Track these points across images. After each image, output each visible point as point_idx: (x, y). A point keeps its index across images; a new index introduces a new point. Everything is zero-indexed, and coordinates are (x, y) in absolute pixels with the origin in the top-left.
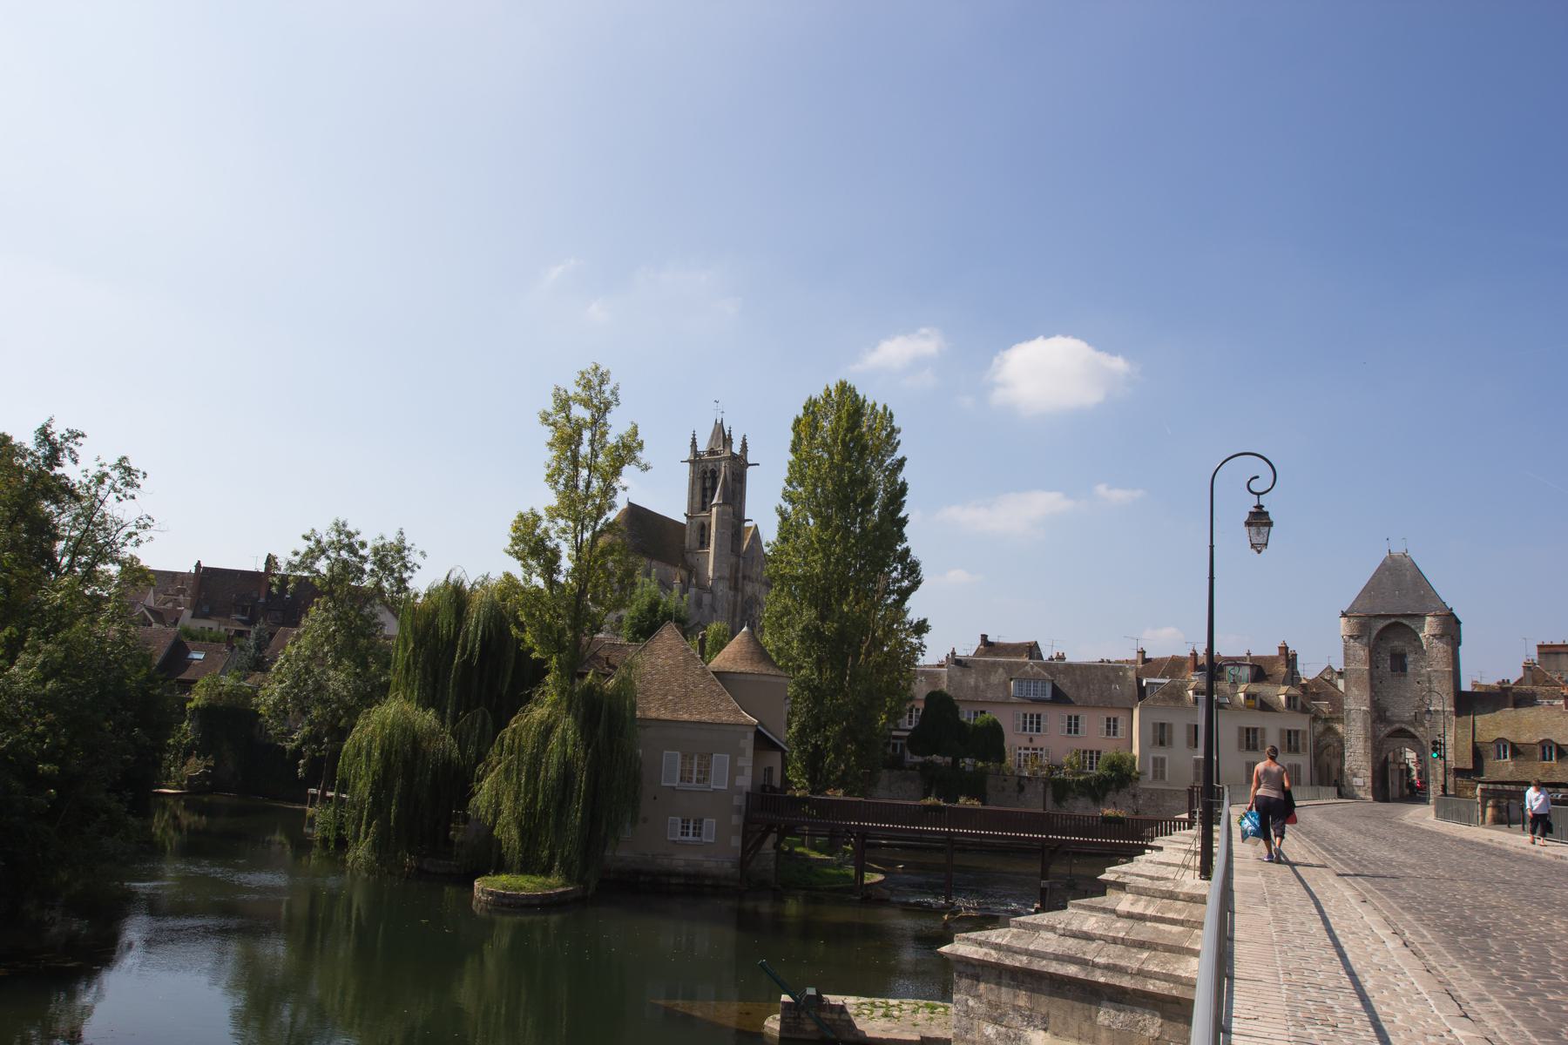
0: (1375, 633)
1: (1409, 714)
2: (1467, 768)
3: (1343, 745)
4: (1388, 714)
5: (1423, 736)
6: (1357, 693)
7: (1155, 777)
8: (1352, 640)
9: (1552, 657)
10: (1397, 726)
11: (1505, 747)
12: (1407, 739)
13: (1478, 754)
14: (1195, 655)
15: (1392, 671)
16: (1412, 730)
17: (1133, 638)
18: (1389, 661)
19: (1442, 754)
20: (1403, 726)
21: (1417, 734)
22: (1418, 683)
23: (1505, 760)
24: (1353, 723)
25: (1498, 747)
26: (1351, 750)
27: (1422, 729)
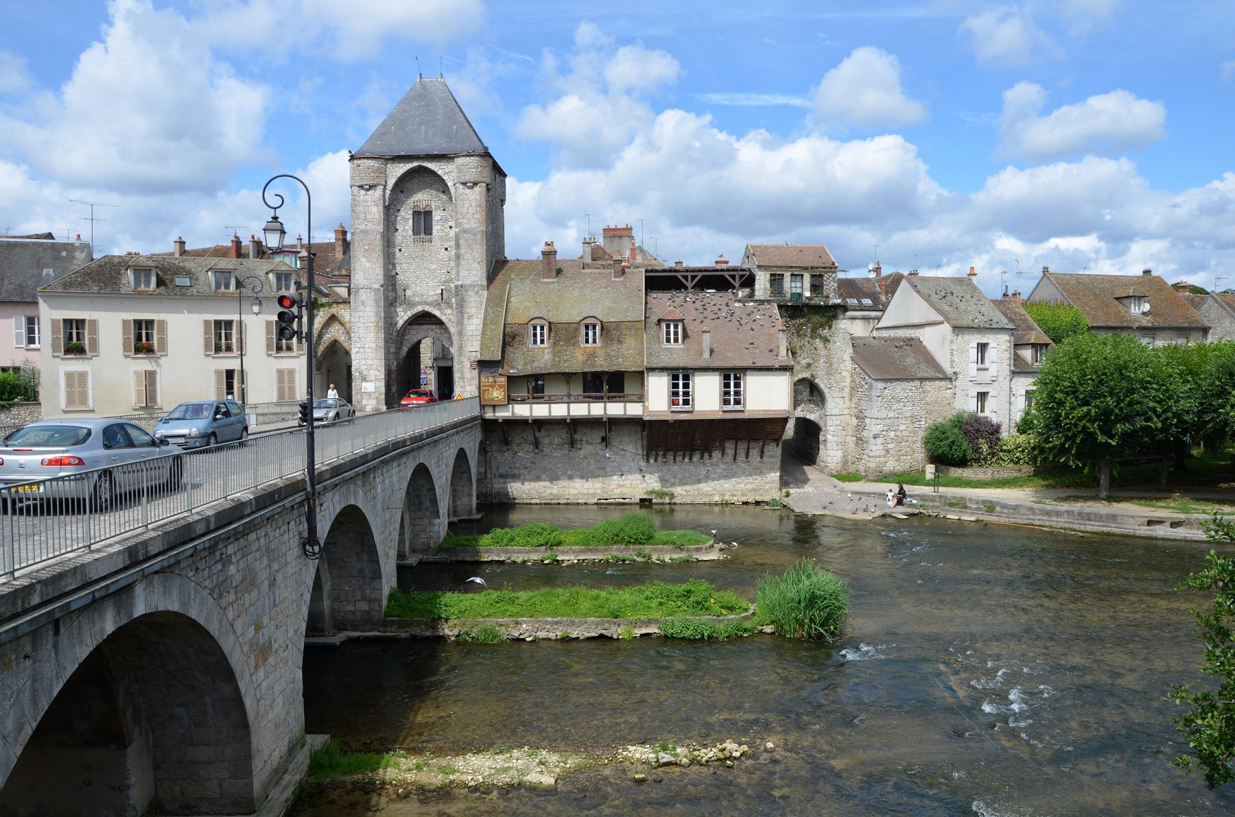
0: (391, 182)
1: (433, 293)
2: (495, 359)
3: (350, 339)
4: (408, 293)
5: (450, 320)
6: (367, 265)
7: (70, 401)
8: (363, 192)
9: (616, 240)
10: (419, 308)
11: (542, 328)
12: (434, 327)
13: (509, 339)
14: (238, 243)
15: (416, 232)
16: (437, 313)
17: (85, 203)
18: (411, 221)
19: (305, 329)
20: (427, 308)
21: (443, 318)
22: (446, 249)
23: (542, 346)
24: (361, 308)
25: (535, 328)
26: (358, 345)
27: (449, 311)
